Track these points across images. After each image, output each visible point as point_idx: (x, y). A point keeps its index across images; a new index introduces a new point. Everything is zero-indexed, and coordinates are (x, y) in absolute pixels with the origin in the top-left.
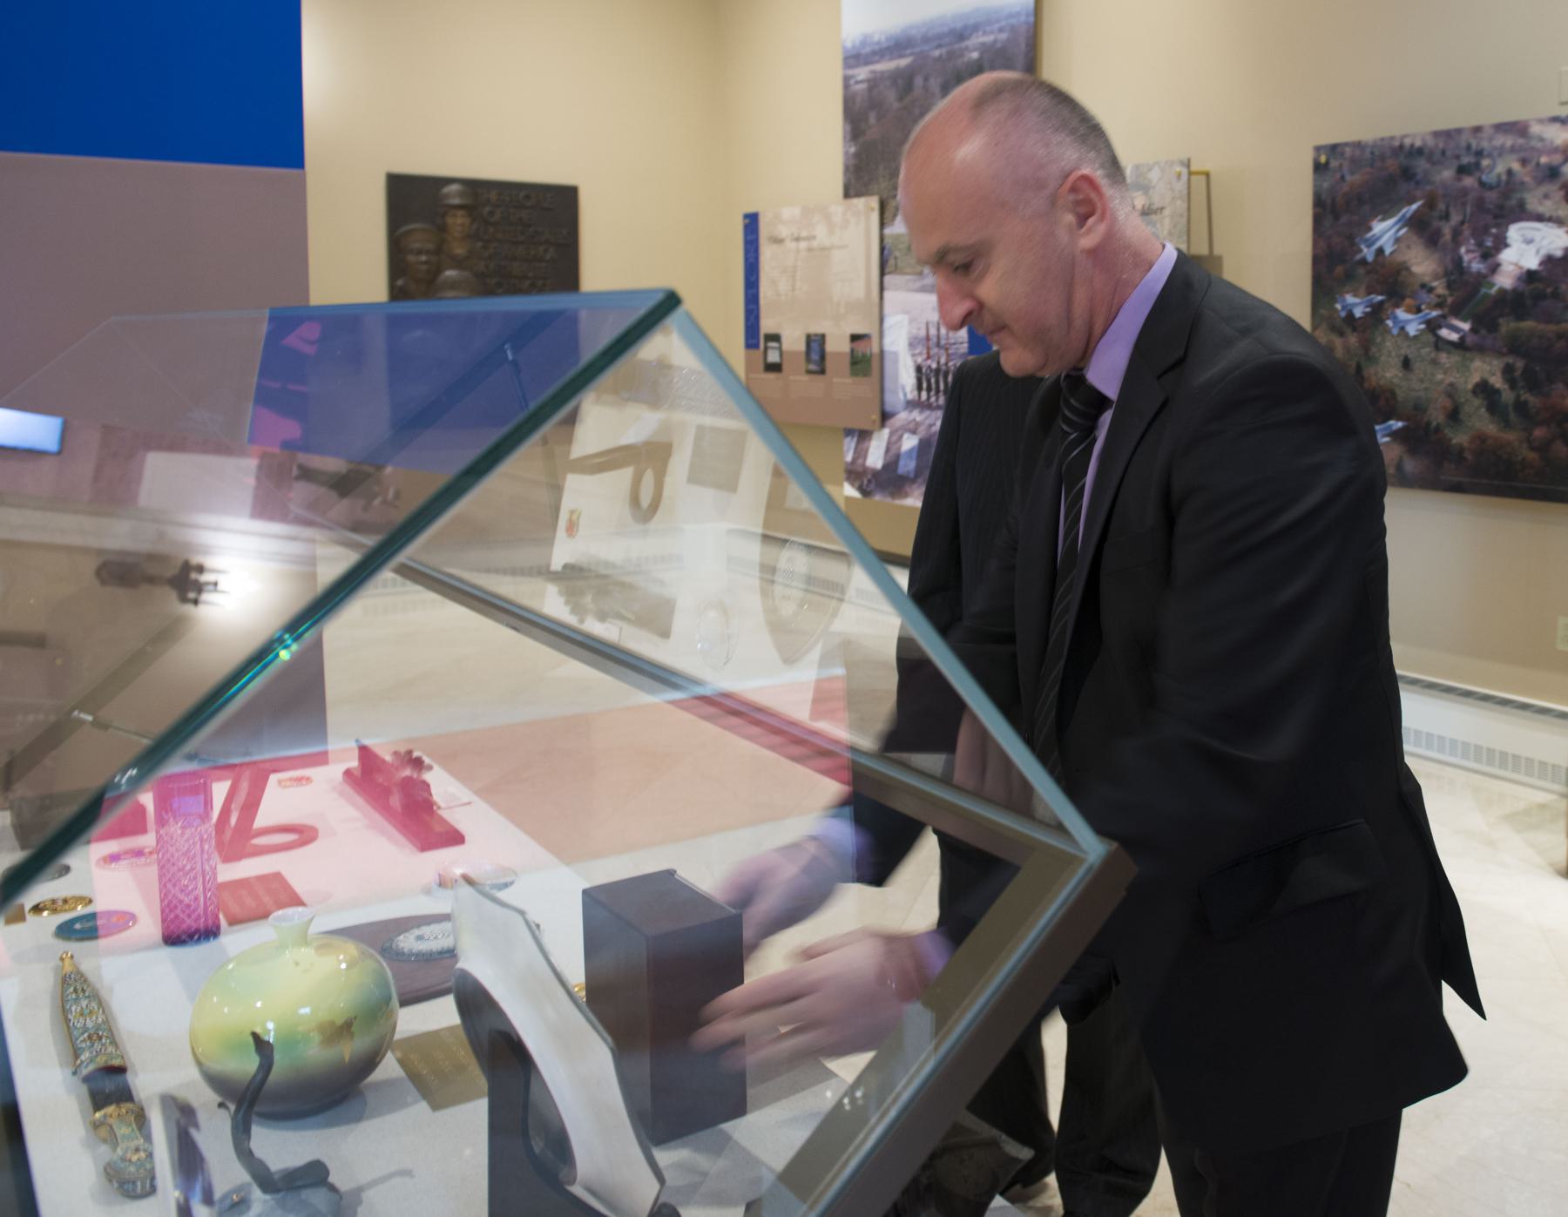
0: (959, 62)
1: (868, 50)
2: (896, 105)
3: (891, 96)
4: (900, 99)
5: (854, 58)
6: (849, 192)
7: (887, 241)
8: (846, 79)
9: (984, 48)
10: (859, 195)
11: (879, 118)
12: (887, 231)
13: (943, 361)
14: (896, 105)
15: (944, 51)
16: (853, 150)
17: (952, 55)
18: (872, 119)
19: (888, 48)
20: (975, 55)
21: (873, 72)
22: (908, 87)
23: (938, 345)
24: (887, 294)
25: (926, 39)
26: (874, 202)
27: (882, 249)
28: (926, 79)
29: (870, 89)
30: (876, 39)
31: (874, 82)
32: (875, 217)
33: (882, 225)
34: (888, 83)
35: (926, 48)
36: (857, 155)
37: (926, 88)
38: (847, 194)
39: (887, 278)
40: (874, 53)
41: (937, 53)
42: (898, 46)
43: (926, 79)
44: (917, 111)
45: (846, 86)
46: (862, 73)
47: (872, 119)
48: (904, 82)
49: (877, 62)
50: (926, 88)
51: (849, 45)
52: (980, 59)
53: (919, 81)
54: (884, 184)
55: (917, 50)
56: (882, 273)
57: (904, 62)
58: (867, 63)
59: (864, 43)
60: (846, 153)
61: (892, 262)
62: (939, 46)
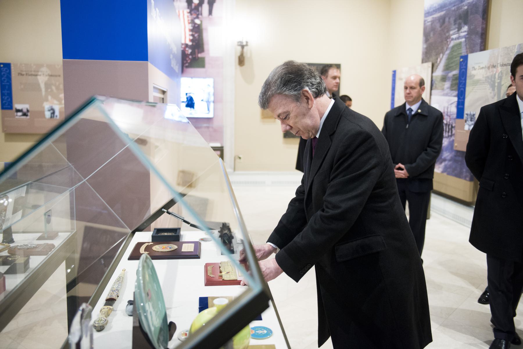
0: (460, 11)
1: (432, 10)
2: (439, 29)
3: (438, 26)
4: (441, 27)
5: (428, 14)
6: (423, 61)
7: (434, 78)
8: (425, 21)
9: (469, 5)
10: (426, 62)
11: (434, 34)
12: (434, 74)
13: (448, 120)
14: (439, 29)
15: (456, 7)
16: (425, 46)
17: (458, 9)
18: (432, 35)
19: (438, 9)
20: (466, 7)
21: (433, 18)
22: (444, 22)
23: (447, 115)
24: (433, 97)
25: (450, 4)
26: (430, 64)
27: (432, 81)
28: (449, 19)
29: (432, 24)
30: (434, 6)
31: (433, 22)
32: (430, 69)
33: (432, 72)
34: (437, 21)
35: (450, 7)
36: (427, 48)
37: (449, 22)
38: (423, 62)
39: (433, 91)
40: (434, 11)
41: (453, 8)
42: (441, 7)
43: (449, 19)
44: (446, 31)
45: (425, 24)
46: (430, 19)
47: (432, 35)
48: (442, 20)
49: (434, 14)
50: (449, 22)
51: (426, 9)
52: (467, 9)
53: (447, 20)
54: (433, 58)
55: (447, 8)
56: (431, 89)
57: (442, 13)
58: (431, 15)
59: (431, 8)
60: (423, 48)
61: (434, 85)
62: (454, 6)
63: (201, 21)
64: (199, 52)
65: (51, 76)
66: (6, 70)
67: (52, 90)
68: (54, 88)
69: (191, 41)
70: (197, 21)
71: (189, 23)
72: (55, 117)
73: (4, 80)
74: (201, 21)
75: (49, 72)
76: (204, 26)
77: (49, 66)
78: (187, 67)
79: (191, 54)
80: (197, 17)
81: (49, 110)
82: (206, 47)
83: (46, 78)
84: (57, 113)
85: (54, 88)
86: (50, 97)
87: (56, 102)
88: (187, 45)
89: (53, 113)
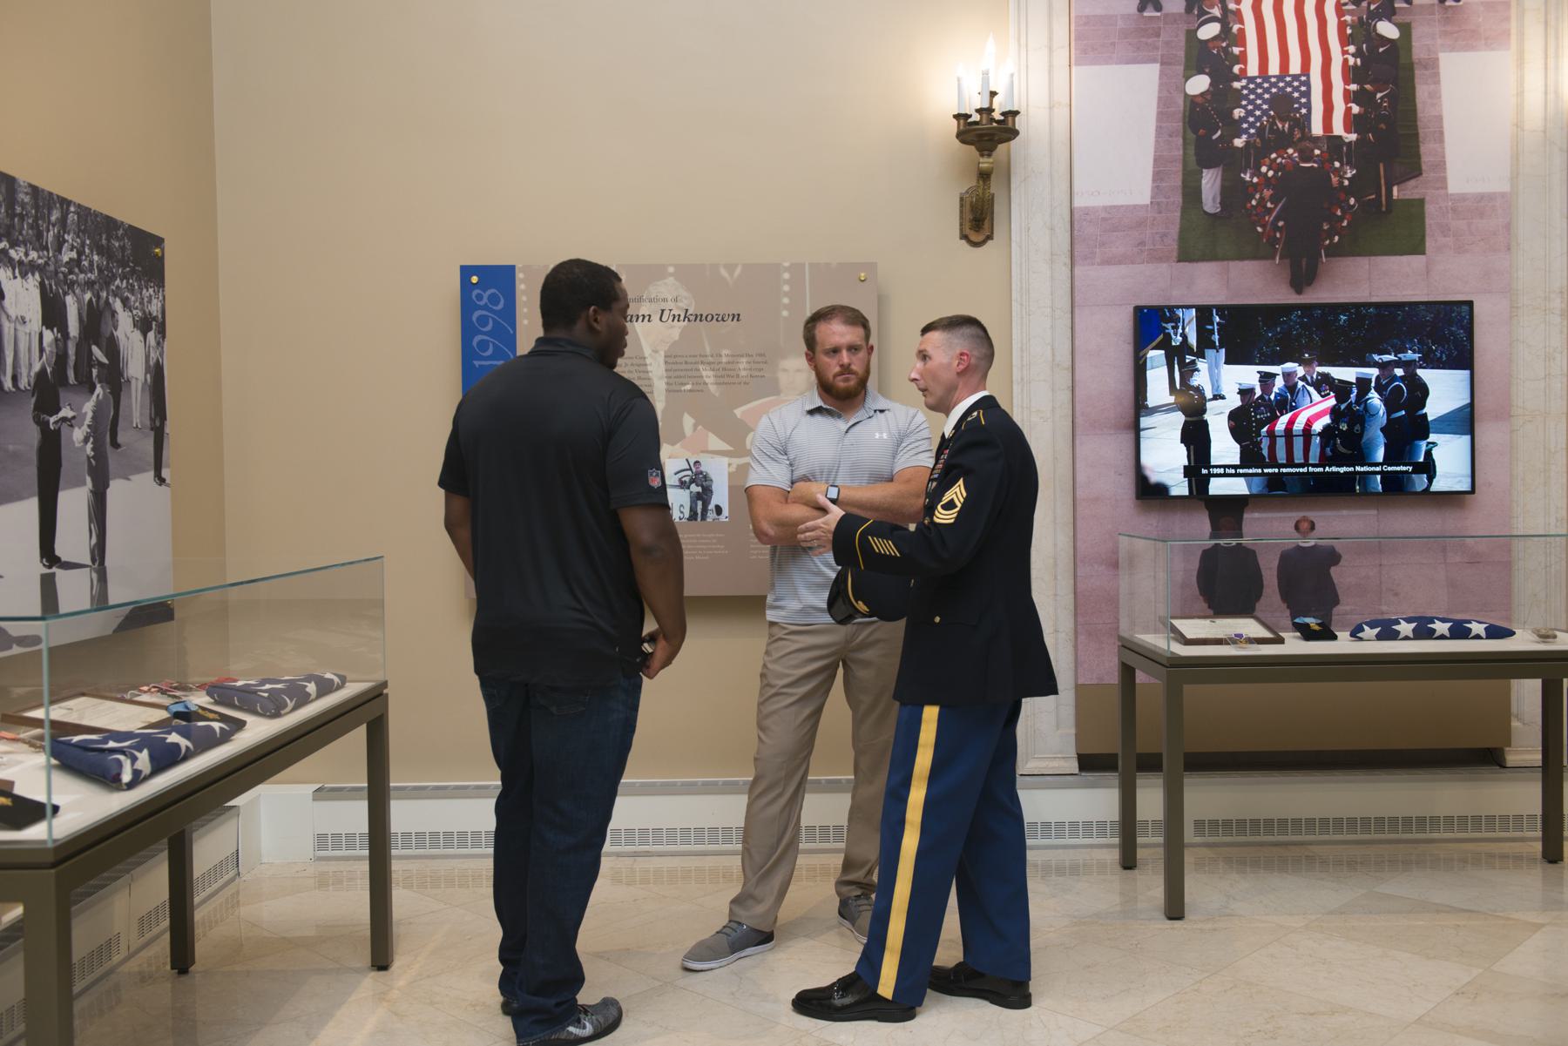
63: (1405, 29)
64: (1402, 180)
65: (699, 317)
66: (494, 299)
67: (700, 387)
68: (708, 375)
69: (1351, 122)
70: (1387, 29)
71: (1344, 40)
72: (711, 515)
73: (483, 345)
74: (1405, 29)
75: (688, 303)
76: (1419, 50)
77: (688, 274)
78: (1335, 252)
79: (1356, 186)
80: (1388, 12)
81: (683, 485)
82: (1426, 149)
83: (675, 330)
84: (720, 496)
85: (708, 375)
86: (688, 422)
87: (715, 442)
88: (1334, 143)
89: (704, 495)
